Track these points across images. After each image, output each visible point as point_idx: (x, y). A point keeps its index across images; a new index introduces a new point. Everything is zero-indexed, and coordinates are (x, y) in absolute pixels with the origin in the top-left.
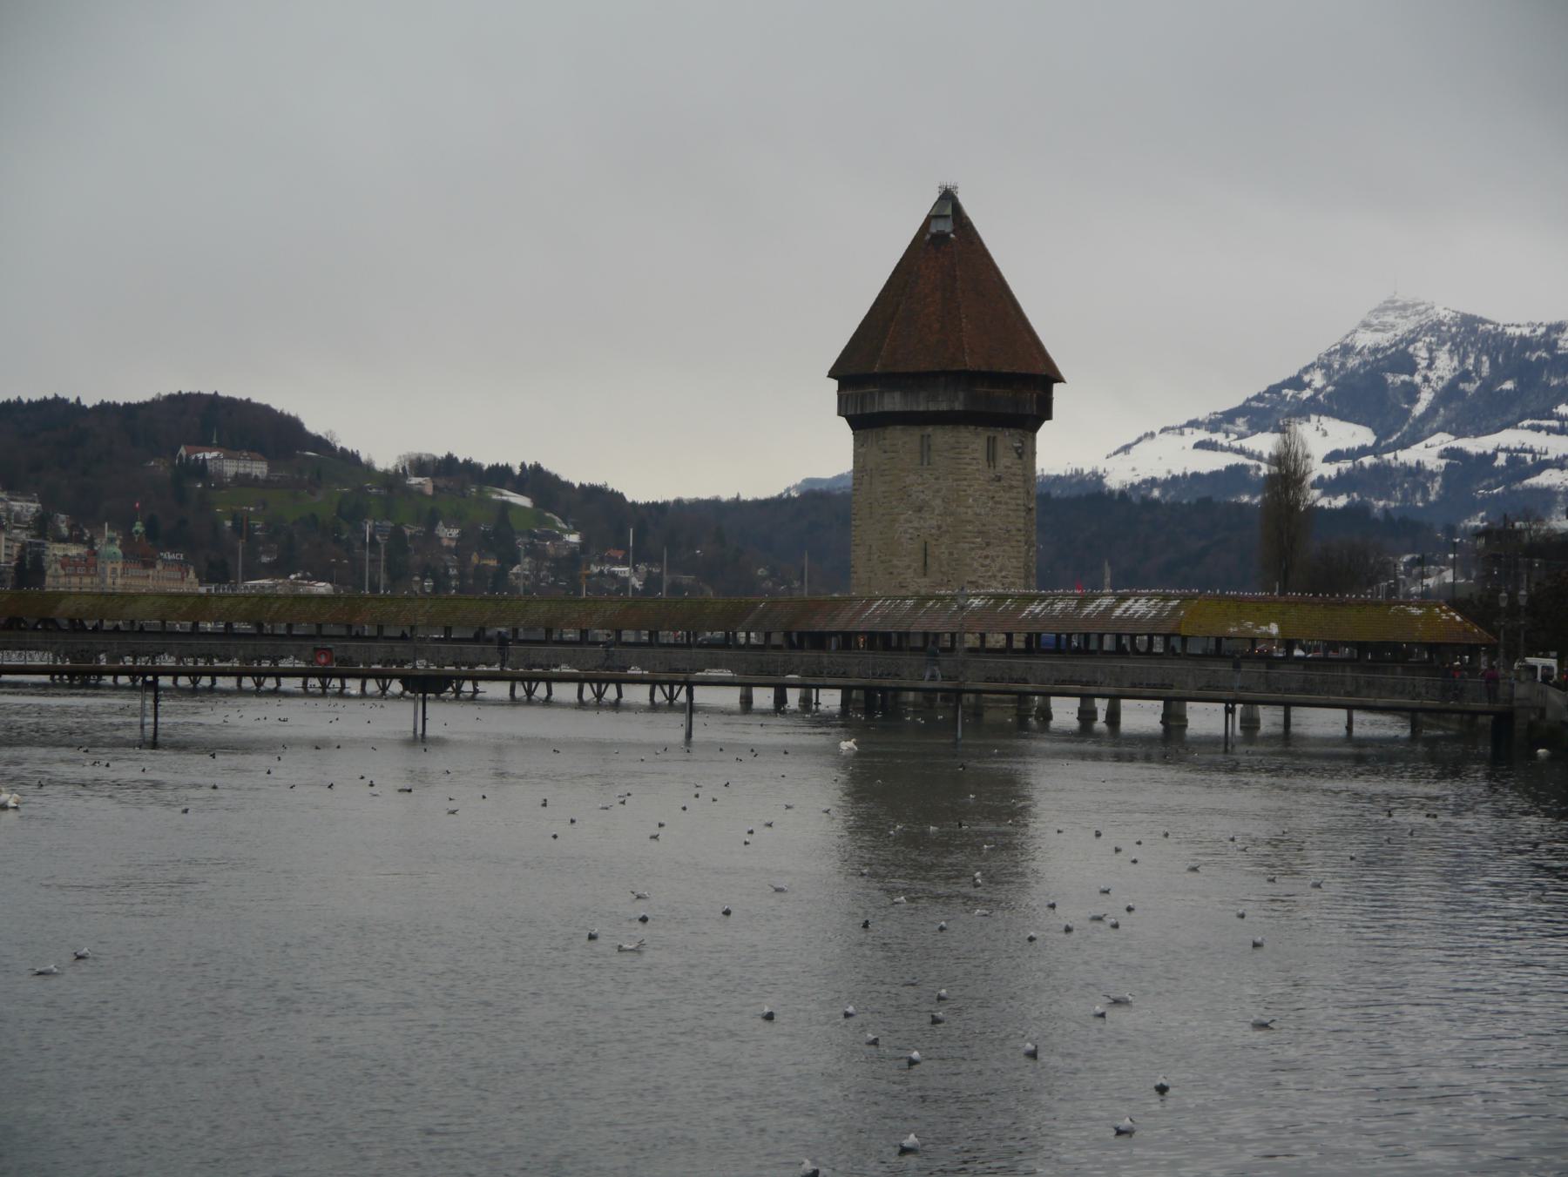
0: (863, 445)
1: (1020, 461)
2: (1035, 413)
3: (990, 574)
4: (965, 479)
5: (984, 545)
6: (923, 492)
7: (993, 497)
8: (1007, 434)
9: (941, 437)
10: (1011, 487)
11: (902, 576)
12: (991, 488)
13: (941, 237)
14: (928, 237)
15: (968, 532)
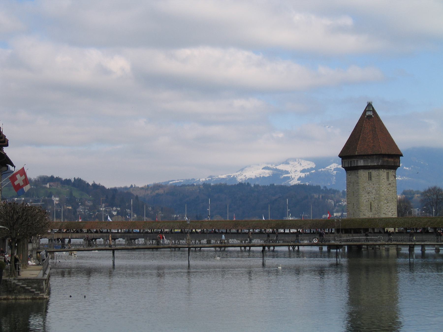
0: (350, 175)
4: (381, 184)
6: (369, 188)
7: (389, 189)
9: (374, 173)
10: (393, 186)
12: (388, 187)
13: (370, 117)
14: (366, 116)
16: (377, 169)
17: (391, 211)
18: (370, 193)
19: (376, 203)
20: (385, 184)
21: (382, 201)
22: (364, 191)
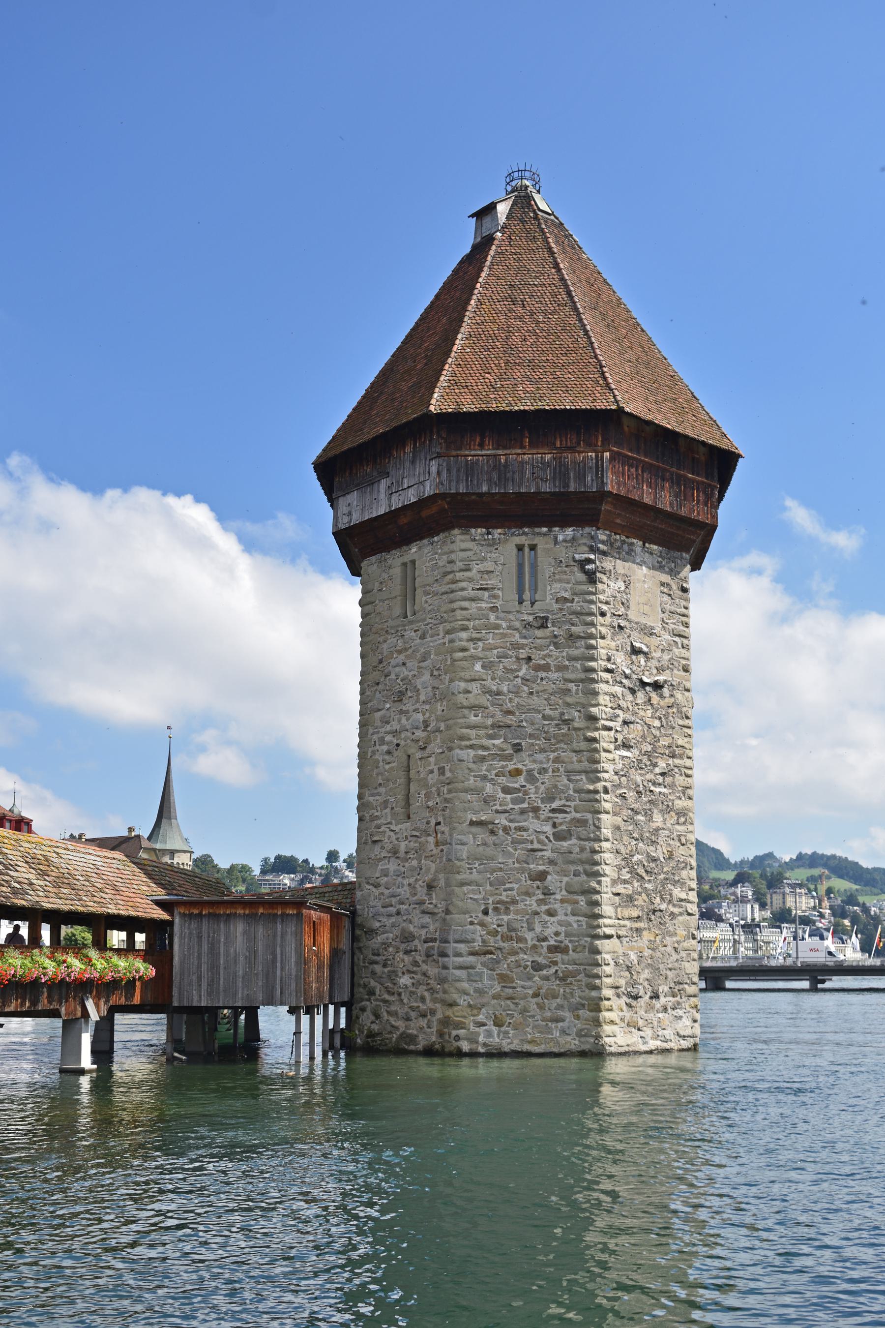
3: (525, 805)
4: (465, 629)
5: (510, 751)
6: (404, 664)
7: (529, 659)
12: (524, 641)
15: (468, 727)
16: (441, 535)
17: (545, 809)
18: (409, 694)
19: (432, 759)
20: (497, 627)
22: (381, 687)
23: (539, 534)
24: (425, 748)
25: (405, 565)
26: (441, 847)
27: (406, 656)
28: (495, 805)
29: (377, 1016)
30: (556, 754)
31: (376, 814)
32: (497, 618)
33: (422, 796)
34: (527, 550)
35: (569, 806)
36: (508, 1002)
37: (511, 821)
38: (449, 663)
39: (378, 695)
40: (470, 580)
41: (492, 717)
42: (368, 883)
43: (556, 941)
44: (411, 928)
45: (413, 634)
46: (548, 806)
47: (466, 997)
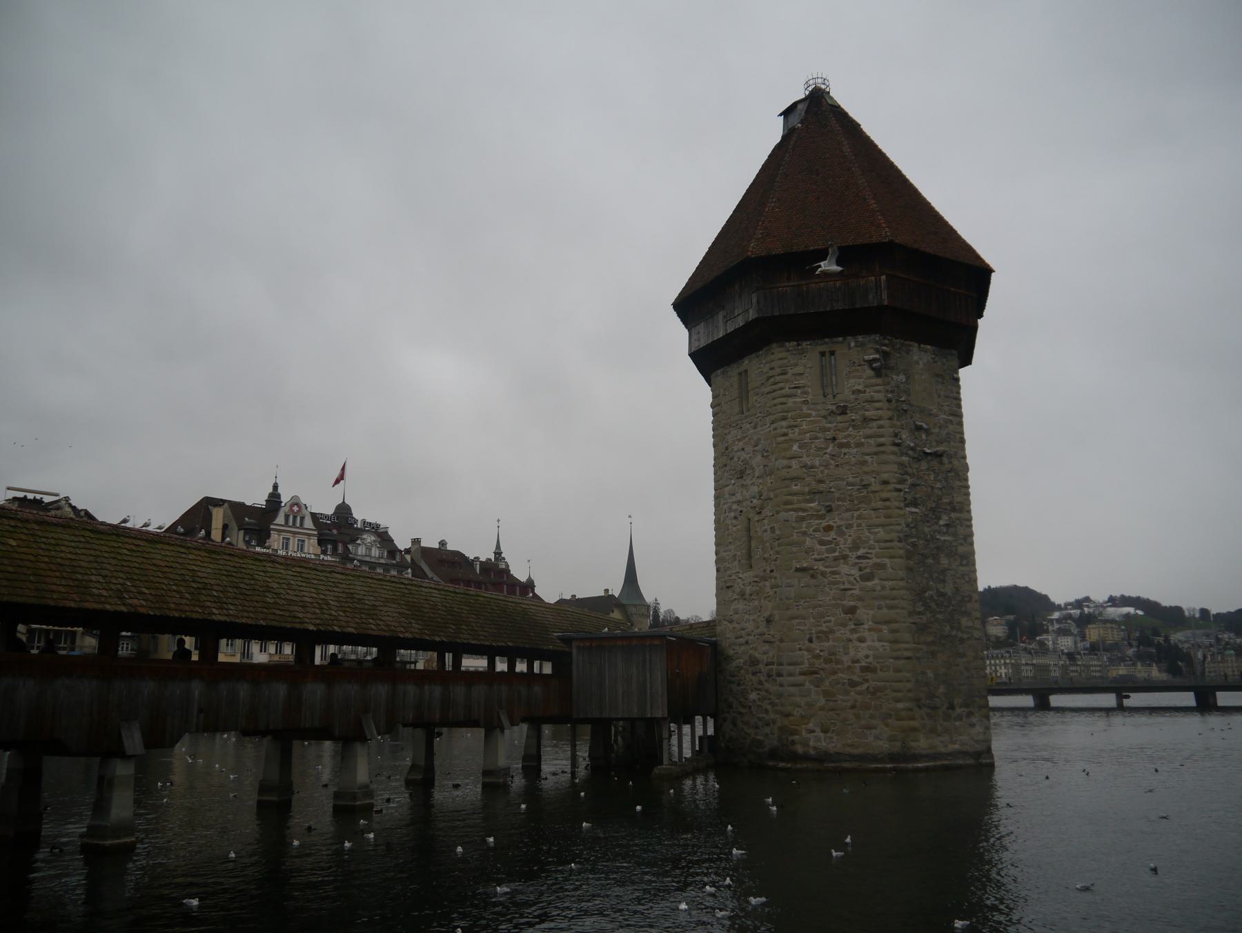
1: (879, 381)
2: (886, 303)
3: (837, 554)
4: (784, 419)
5: (823, 512)
6: (743, 449)
7: (834, 439)
8: (853, 344)
9: (756, 367)
10: (866, 420)
11: (729, 572)
15: (791, 494)
18: (748, 472)
19: (766, 521)
20: (809, 416)
21: (790, 507)
22: (727, 468)
23: (837, 342)
24: (760, 513)
25: (740, 374)
26: (776, 589)
27: (744, 443)
28: (814, 555)
29: (735, 724)
30: (858, 512)
31: (728, 566)
32: (809, 409)
33: (760, 550)
34: (827, 355)
35: (871, 553)
36: (831, 713)
37: (827, 567)
38: (774, 445)
39: (726, 474)
40: (787, 381)
41: (808, 486)
42: (724, 620)
43: (866, 662)
44: (757, 655)
45: (748, 426)
46: (855, 553)
47: (799, 709)
